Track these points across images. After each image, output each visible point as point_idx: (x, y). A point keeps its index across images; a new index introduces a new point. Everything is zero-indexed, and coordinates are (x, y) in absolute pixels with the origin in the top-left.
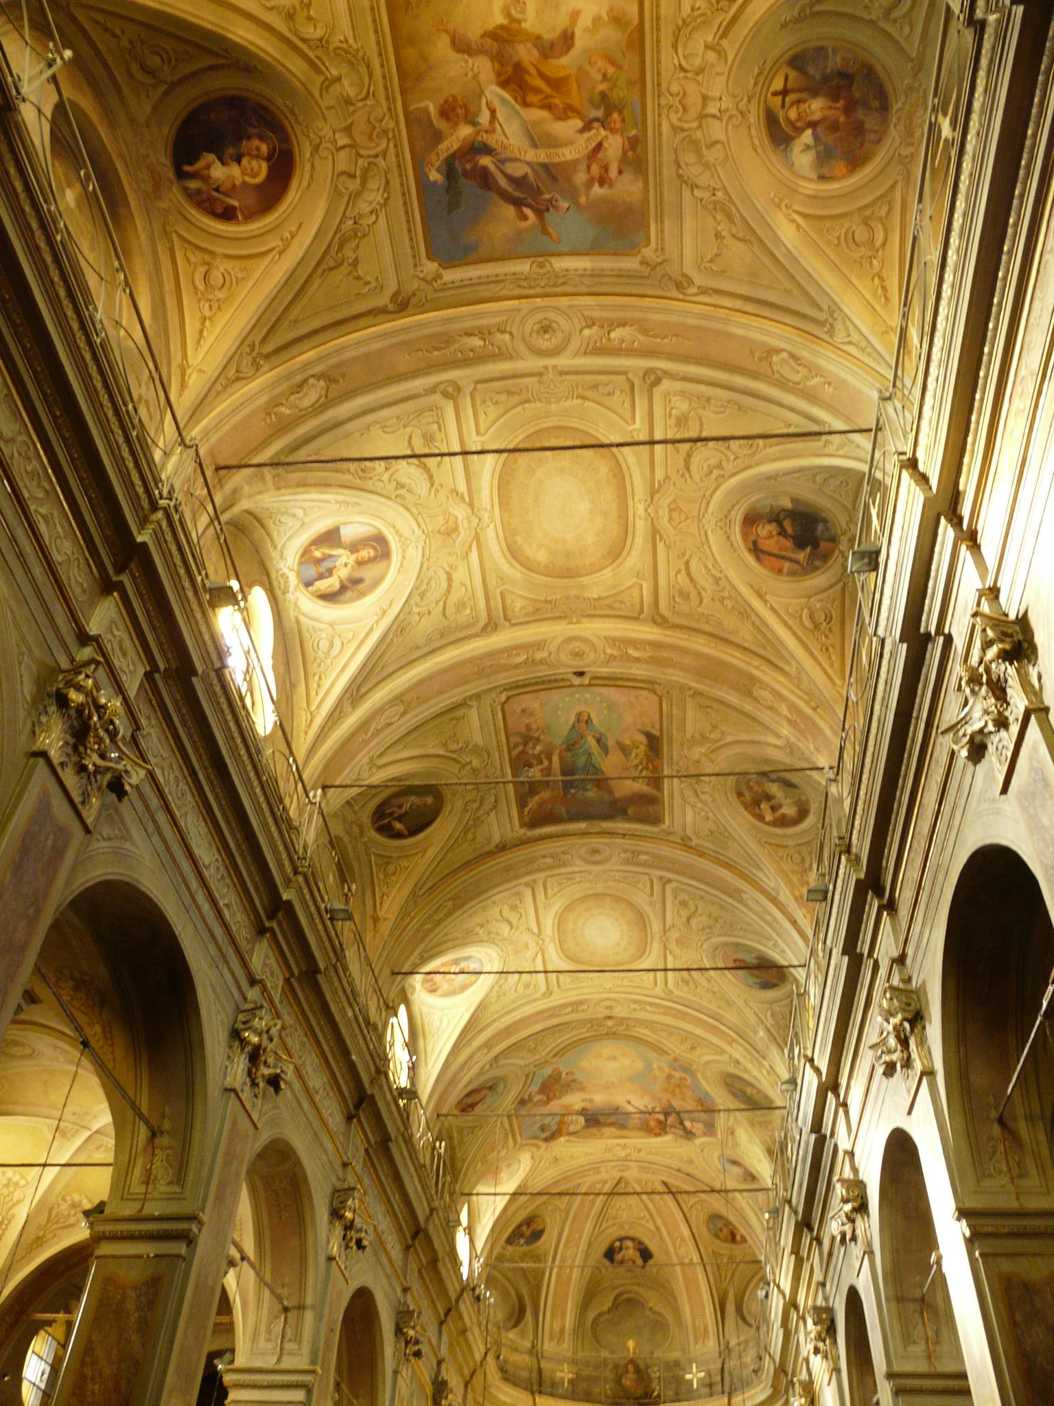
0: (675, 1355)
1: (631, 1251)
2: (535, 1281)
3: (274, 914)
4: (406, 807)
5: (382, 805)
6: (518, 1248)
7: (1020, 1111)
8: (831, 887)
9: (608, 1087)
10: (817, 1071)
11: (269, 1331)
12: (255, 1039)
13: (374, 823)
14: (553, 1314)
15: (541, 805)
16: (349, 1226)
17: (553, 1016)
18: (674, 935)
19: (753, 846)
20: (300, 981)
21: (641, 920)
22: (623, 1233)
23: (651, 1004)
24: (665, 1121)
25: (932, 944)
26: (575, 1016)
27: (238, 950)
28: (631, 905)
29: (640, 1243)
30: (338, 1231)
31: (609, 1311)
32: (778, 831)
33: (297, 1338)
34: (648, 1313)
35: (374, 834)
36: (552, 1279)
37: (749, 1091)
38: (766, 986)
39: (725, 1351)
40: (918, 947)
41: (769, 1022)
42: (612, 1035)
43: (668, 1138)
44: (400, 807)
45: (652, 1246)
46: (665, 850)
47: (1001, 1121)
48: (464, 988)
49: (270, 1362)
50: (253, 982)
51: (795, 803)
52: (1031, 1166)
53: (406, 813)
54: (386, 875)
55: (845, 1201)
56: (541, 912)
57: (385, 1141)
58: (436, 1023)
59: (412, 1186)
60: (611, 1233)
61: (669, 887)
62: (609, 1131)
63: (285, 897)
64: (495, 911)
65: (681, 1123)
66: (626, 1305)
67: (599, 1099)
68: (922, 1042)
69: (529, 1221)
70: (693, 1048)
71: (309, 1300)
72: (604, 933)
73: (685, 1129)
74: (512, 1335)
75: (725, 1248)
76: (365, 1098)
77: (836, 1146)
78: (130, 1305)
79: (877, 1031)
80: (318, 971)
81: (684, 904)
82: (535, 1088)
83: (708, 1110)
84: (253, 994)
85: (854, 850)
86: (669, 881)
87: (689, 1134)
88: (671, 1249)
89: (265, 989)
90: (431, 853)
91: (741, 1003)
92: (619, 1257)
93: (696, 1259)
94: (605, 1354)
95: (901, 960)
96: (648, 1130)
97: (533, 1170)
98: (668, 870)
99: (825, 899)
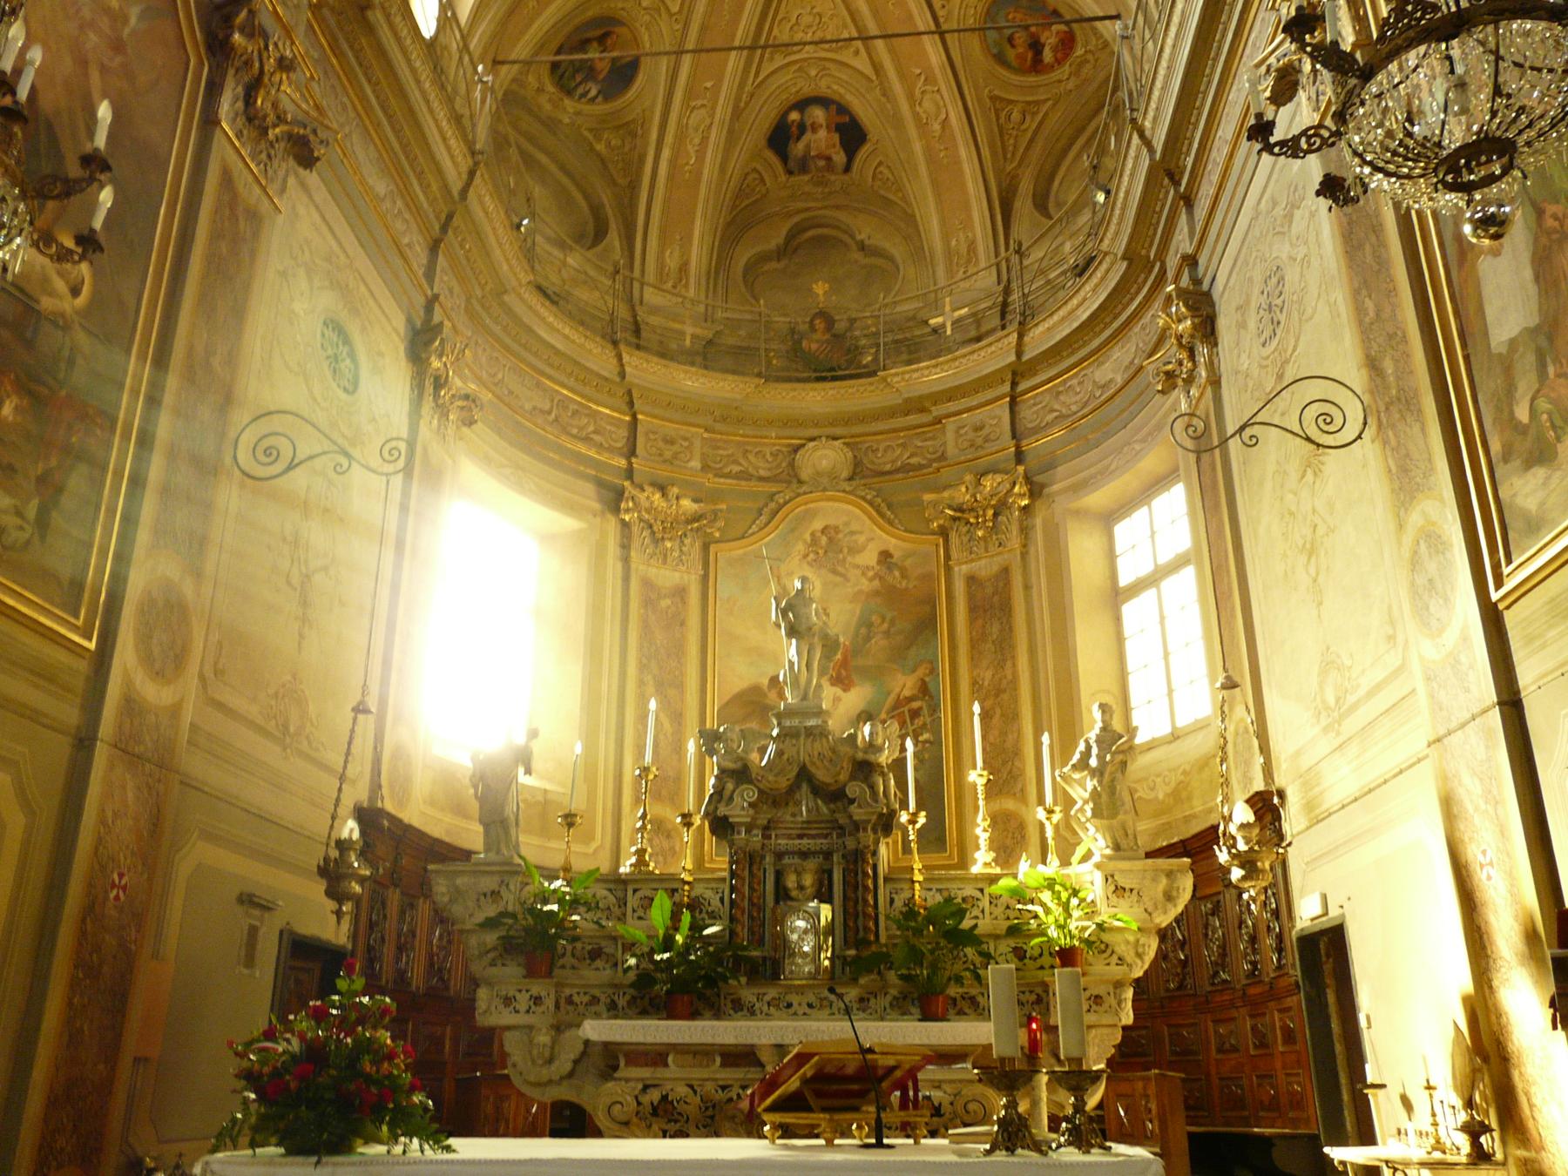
1: (822, 133)
6: (587, 108)
29: (842, 109)
34: (856, 255)
36: (658, 167)
45: (865, 112)
66: (808, 244)
92: (798, 149)
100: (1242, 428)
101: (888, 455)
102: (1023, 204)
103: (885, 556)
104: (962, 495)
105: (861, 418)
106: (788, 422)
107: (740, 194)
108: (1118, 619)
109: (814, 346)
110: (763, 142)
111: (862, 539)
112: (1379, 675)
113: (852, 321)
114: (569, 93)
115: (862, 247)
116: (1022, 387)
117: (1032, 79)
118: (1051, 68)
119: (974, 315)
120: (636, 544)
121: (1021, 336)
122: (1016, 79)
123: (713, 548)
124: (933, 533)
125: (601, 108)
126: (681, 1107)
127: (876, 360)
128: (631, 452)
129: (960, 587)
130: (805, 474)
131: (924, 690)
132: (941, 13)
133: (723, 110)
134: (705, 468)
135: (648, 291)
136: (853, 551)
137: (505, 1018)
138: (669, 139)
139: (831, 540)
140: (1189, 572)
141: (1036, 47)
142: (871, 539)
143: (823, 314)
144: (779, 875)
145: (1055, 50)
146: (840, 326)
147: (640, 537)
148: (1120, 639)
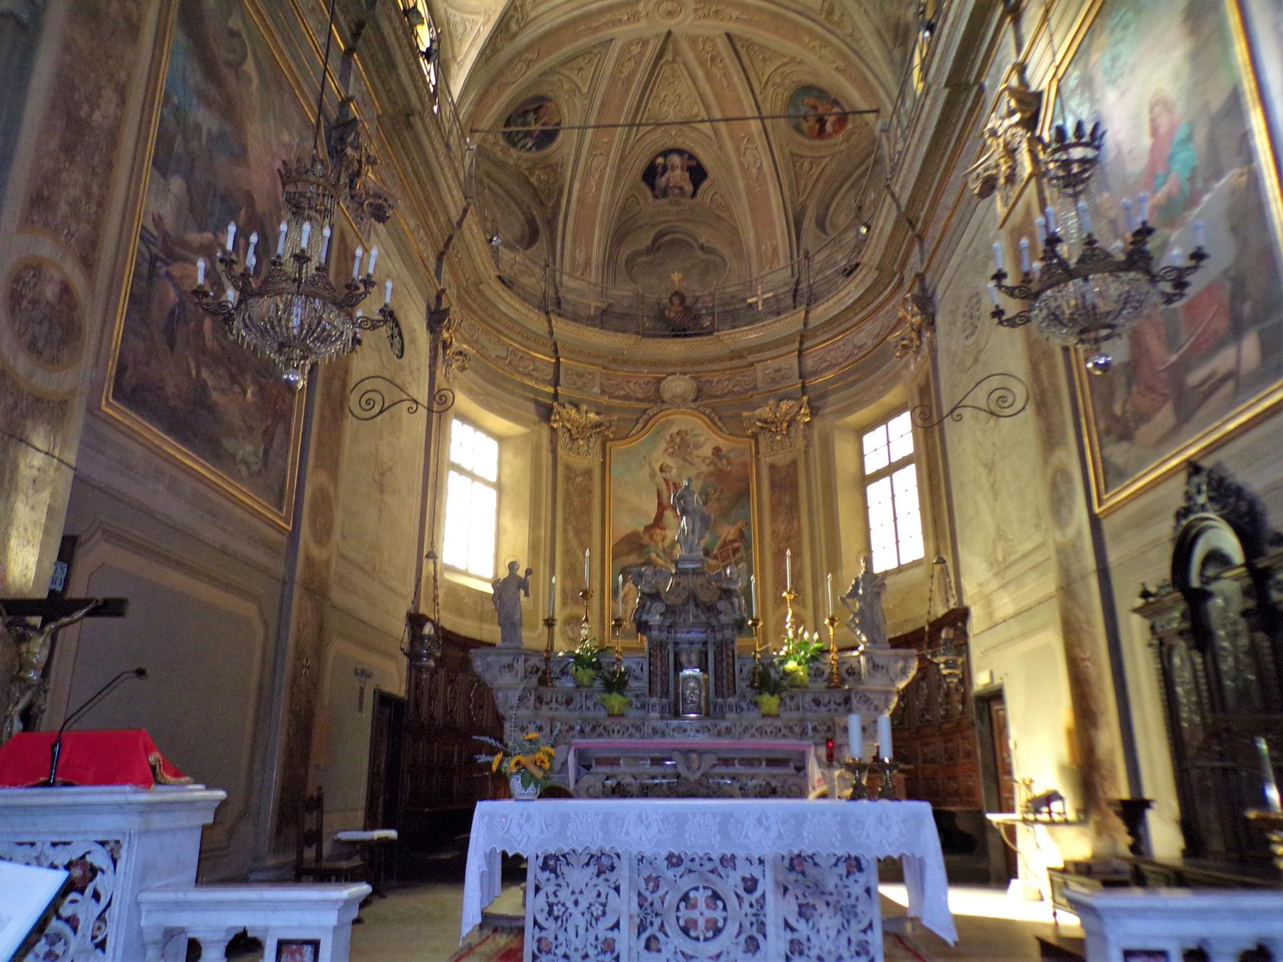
1: (678, 172)
6: (529, 155)
29: (692, 157)
34: (699, 253)
45: (706, 159)
92: (661, 182)
100: (952, 411)
102: (809, 224)
103: (717, 450)
104: (765, 412)
105: (701, 362)
106: (654, 363)
107: (624, 208)
108: (864, 495)
109: (672, 315)
110: (639, 177)
111: (702, 439)
112: (1028, 546)
113: (697, 299)
114: (514, 145)
115: (702, 248)
116: (806, 345)
117: (817, 143)
118: (830, 136)
119: (774, 296)
120: (561, 442)
121: (807, 313)
122: (807, 142)
123: (608, 444)
124: (748, 436)
125: (534, 155)
126: (628, 789)
127: (712, 324)
128: (556, 383)
130: (666, 396)
131: (743, 536)
132: (760, 98)
133: (613, 157)
134: (603, 392)
135: (565, 278)
138: (579, 176)
139: (682, 439)
140: (911, 470)
141: (821, 121)
142: (708, 439)
143: (677, 293)
144: (676, 655)
145: (834, 124)
146: (689, 301)
147: (563, 439)
148: (865, 508)
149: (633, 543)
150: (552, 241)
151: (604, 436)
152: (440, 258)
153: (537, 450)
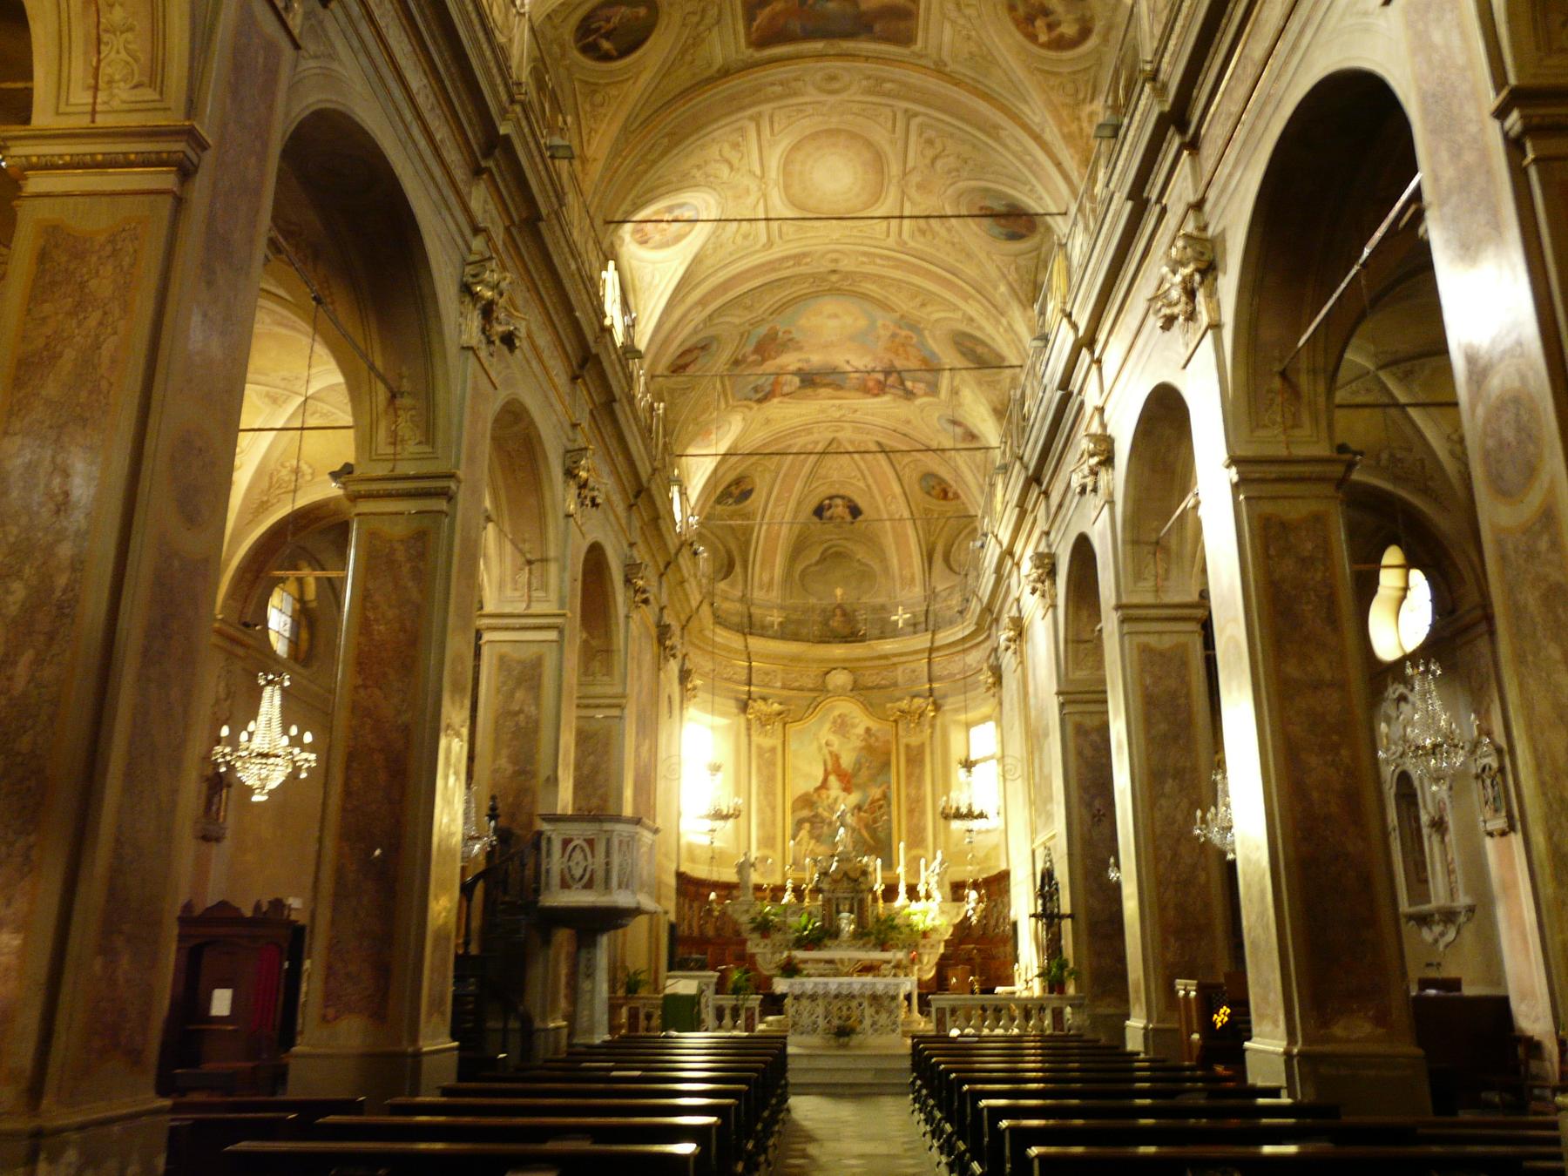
0: (880, 600)
2: (744, 538)
3: (491, 152)
4: (615, 20)
5: (586, 19)
7: (1304, 363)
8: (1126, 121)
9: (826, 346)
10: (1075, 327)
11: (515, 582)
12: (489, 294)
13: (577, 41)
14: (762, 564)
15: (773, 18)
16: (583, 485)
17: (774, 270)
18: (915, 178)
19: (1020, 73)
20: (520, 231)
21: (878, 161)
22: (833, 492)
23: (882, 257)
24: (889, 381)
25: (1242, 188)
26: (797, 270)
27: (458, 192)
28: (869, 144)
29: (850, 500)
30: (574, 491)
31: (817, 563)
32: (1052, 54)
33: (544, 586)
35: (576, 54)
36: (761, 534)
37: (980, 349)
38: (1014, 237)
39: (931, 595)
40: (1223, 191)
41: (1013, 277)
42: (835, 291)
43: (886, 398)
44: (608, 20)
45: (862, 503)
46: (915, 78)
47: (1283, 375)
48: (678, 239)
49: (520, 608)
50: (477, 230)
51: (1078, 20)
52: (1306, 418)
53: (615, 29)
54: (593, 105)
55: (1092, 455)
56: (765, 153)
57: (610, 400)
58: (648, 278)
59: (636, 446)
60: (821, 492)
61: (915, 122)
62: (823, 391)
63: (502, 131)
64: (713, 151)
65: (902, 383)
66: (834, 557)
67: (816, 359)
68: (1212, 294)
69: (738, 482)
70: (923, 305)
71: (552, 553)
72: (835, 176)
73: (906, 390)
74: (722, 585)
75: (937, 505)
76: (590, 358)
77: (1082, 404)
78: (400, 556)
79: (1155, 283)
80: (539, 218)
81: (930, 142)
82: (749, 348)
83: (932, 368)
84: (478, 243)
85: (1162, 76)
86: (916, 115)
87: (909, 395)
88: (882, 506)
89: (489, 239)
90: (645, 77)
91: (983, 256)
92: (828, 514)
93: (906, 514)
94: (812, 601)
95: (1198, 206)
96: (865, 390)
97: (744, 432)
98: (915, 101)
99: (1115, 135)
101: (870, 679)
103: (868, 730)
104: (904, 704)
106: (822, 661)
125: (734, 507)
128: (749, 683)
129: (902, 750)
130: (830, 687)
133: (792, 504)
136: (854, 726)
137: (754, 950)
142: (861, 721)
147: (755, 725)
149: (806, 801)
150: (745, 567)
151: (784, 718)
152: (683, 628)
153: (737, 736)
